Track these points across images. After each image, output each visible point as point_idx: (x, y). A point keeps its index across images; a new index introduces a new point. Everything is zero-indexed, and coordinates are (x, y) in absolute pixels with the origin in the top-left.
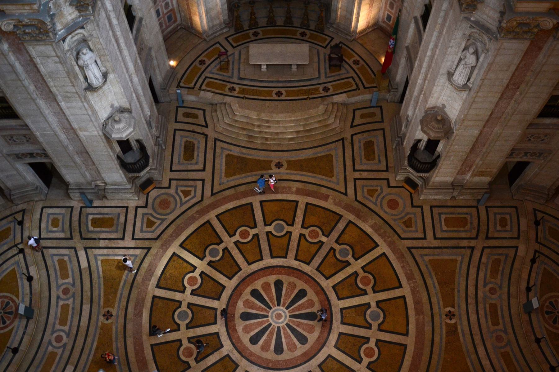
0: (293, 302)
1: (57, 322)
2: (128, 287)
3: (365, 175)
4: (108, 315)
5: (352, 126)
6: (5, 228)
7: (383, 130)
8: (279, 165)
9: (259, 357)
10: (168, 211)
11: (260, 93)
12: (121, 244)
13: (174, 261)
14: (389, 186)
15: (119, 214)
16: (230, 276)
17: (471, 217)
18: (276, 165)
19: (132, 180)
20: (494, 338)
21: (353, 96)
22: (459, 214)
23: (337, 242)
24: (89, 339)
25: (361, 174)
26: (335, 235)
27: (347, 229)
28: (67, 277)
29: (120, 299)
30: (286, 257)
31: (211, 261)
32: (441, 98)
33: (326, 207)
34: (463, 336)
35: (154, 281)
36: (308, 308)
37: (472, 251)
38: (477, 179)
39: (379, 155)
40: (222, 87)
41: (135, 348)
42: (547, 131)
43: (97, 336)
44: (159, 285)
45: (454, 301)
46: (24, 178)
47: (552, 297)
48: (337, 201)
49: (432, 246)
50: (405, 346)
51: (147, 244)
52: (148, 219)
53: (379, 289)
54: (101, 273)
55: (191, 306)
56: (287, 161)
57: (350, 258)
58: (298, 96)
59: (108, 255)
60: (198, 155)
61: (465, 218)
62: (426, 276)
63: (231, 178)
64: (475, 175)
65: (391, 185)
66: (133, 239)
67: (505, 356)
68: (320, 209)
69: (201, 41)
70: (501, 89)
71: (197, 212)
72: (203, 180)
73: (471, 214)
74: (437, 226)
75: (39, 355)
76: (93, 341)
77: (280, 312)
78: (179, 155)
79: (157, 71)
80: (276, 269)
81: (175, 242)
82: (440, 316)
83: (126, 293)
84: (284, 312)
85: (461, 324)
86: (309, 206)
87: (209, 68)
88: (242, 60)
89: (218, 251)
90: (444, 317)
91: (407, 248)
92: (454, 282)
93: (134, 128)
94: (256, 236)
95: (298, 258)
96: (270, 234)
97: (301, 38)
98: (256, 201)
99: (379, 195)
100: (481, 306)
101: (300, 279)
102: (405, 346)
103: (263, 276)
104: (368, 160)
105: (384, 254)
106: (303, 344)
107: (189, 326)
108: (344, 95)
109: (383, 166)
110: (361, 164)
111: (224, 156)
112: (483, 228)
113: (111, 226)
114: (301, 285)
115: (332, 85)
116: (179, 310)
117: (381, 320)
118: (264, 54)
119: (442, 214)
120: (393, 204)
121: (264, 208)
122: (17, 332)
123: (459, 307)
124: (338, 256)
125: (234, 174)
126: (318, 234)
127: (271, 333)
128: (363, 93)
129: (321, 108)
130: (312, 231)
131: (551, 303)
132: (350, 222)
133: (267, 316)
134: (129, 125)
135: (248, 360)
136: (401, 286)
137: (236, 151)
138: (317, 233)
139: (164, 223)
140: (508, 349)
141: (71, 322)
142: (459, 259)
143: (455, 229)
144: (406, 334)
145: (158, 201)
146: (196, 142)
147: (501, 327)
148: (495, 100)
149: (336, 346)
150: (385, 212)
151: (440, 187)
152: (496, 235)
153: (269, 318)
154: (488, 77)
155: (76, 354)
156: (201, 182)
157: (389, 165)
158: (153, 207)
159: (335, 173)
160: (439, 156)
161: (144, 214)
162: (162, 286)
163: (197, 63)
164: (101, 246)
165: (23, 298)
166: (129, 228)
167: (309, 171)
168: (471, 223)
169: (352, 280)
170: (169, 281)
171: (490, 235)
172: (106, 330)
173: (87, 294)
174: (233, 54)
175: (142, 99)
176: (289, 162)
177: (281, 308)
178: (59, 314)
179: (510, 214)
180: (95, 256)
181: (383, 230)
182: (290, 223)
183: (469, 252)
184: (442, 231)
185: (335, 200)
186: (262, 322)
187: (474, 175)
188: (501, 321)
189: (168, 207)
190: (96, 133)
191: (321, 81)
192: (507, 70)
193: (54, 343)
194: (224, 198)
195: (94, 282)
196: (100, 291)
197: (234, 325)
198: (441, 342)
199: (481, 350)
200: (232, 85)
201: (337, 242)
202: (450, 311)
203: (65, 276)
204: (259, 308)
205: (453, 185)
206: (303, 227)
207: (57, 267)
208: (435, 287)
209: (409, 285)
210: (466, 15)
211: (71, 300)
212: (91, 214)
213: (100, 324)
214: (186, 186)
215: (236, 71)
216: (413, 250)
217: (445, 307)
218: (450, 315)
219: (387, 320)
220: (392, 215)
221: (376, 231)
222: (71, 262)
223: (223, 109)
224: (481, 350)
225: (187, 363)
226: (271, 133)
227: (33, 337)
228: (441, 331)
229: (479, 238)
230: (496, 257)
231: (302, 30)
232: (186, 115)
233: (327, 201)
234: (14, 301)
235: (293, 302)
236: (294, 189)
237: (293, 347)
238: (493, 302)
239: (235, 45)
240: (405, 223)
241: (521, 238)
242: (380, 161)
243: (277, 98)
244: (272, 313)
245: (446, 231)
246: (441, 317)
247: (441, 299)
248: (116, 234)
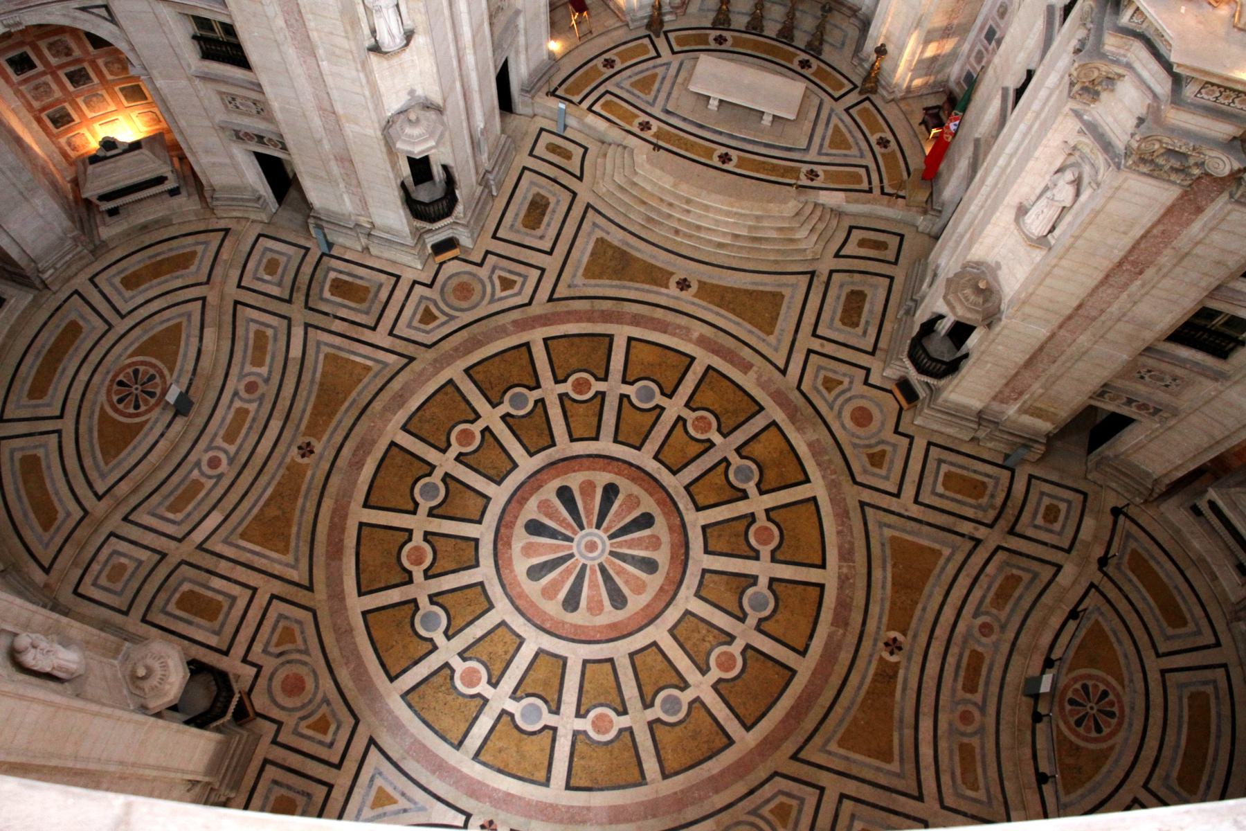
0: (624, 530)
1: (222, 433)
2: (355, 412)
3: (829, 349)
4: (307, 450)
5: (837, 255)
6: (188, 250)
7: (892, 279)
8: (683, 285)
9: (533, 604)
10: (465, 305)
11: (690, 147)
12: (368, 336)
13: (446, 394)
14: (866, 383)
15: (381, 286)
16: (532, 450)
17: (996, 486)
18: (678, 283)
19: (419, 236)
20: (957, 714)
21: (856, 201)
22: (975, 472)
23: (738, 450)
24: (264, 479)
25: (822, 345)
26: (739, 437)
28: (261, 364)
29: (335, 429)
30: (639, 448)
31: (508, 414)
32: (996, 250)
33: (740, 383)
34: (904, 689)
35: (401, 416)
36: (647, 548)
37: (975, 547)
38: (1026, 419)
39: (867, 322)
40: (629, 118)
41: (332, 518)
42: (1179, 372)
43: (278, 478)
44: (408, 427)
45: (909, 624)
46: (241, 174)
47: (1090, 677)
48: (765, 378)
49: (906, 514)
50: (794, 672)
51: (410, 349)
52: (427, 310)
53: (782, 558)
54: (318, 375)
55: (448, 480)
56: (699, 282)
57: (751, 487)
58: (758, 171)
59: (339, 348)
60: (548, 225)
61: (983, 483)
62: (876, 563)
63: (593, 282)
64: (1026, 412)
65: (871, 381)
66: (391, 334)
67: (966, 753)
68: (728, 383)
69: (619, 24)
70: (1106, 265)
71: (515, 322)
72: (543, 270)
73: (997, 480)
74: (928, 481)
75: (175, 479)
76: (269, 484)
77: (596, 539)
78: (517, 215)
79: (522, 57)
80: (615, 463)
81: (458, 362)
82: (876, 640)
83: (348, 423)
84: (603, 543)
85: (907, 669)
86: (711, 371)
87: (617, 78)
88: (680, 80)
89: (525, 400)
90: (881, 645)
91: (860, 502)
92: (921, 591)
93: (438, 143)
94: (601, 395)
95: (660, 457)
96: (625, 400)
97: (799, 69)
98: (621, 333)
99: (844, 392)
100: (954, 650)
101: (651, 495)
102: (794, 672)
103: (589, 469)
104: (844, 324)
105: (814, 499)
106: (616, 608)
107: (435, 512)
108: (841, 195)
109: (868, 344)
110: (830, 326)
111: (594, 239)
112: (1011, 512)
113: (362, 300)
114: (648, 504)
115: (825, 171)
116: (427, 480)
117: (767, 613)
118: (719, 79)
119: (944, 462)
120: (862, 418)
121: (632, 351)
122: (152, 428)
123: (915, 636)
124: (731, 477)
125: (600, 276)
126: (710, 428)
127: (569, 571)
128: (875, 201)
129: (791, 206)
130: (702, 418)
131: (1085, 687)
132: (774, 423)
133: (571, 540)
134: (431, 134)
135: (513, 603)
136: (823, 566)
137: (616, 237)
138: (710, 424)
139: (452, 323)
140: (975, 741)
141: (244, 440)
142: (946, 552)
143: (959, 497)
144: (803, 653)
145: (455, 281)
146: (552, 200)
147: (977, 698)
148: (1091, 283)
149: (672, 631)
150: (843, 427)
151: (956, 414)
152: (1030, 532)
153: (574, 544)
154: (1086, 234)
155: (233, 497)
156: (539, 272)
157: (880, 345)
158: (442, 291)
159: (777, 331)
160: (966, 356)
161: (422, 298)
162: (412, 430)
163: (599, 62)
164: (333, 328)
165: (179, 376)
166: (391, 313)
167: (733, 311)
168: (992, 496)
169: (741, 526)
170: (427, 426)
171: (1018, 529)
172: (294, 474)
173: (284, 403)
174: (668, 64)
175: (476, 97)
176: (702, 284)
177: (600, 532)
178: (228, 421)
179: (1069, 502)
180: (319, 343)
181: (826, 458)
182: (668, 392)
183: (970, 544)
184: (934, 493)
185: (760, 376)
186: (558, 546)
187: (1023, 411)
188: (981, 689)
189: (466, 298)
190: (370, 132)
191: (807, 158)
192: (1125, 233)
193: (205, 468)
194: (568, 313)
195: (302, 386)
196: (306, 406)
197: (510, 537)
198: (859, 688)
199: (926, 724)
200: (647, 118)
201: (738, 450)
202: (895, 640)
203: (258, 362)
204: (562, 522)
205: (980, 418)
206: (687, 405)
207: (251, 342)
208: (883, 587)
209: (840, 567)
210: (1077, 107)
211: (255, 405)
212: (335, 270)
213: (288, 460)
214: (510, 272)
215: (663, 95)
216: (867, 509)
217: (889, 629)
218: (893, 646)
219: (778, 616)
220: (853, 435)
221: (814, 455)
222: (275, 339)
223: (618, 155)
224: (926, 724)
225: (410, 573)
226: (688, 224)
227: (175, 448)
228: (867, 670)
229: (997, 527)
230: (1015, 572)
231: (807, 57)
232: (553, 148)
233: (746, 373)
234: (162, 376)
235: (624, 530)
236: (696, 335)
237: (595, 608)
238: (980, 649)
239: (676, 48)
240: (871, 457)
241: (1074, 553)
242: (865, 333)
243: (719, 165)
244: (583, 537)
245: (941, 496)
246: (875, 645)
247: (887, 612)
248: (364, 316)
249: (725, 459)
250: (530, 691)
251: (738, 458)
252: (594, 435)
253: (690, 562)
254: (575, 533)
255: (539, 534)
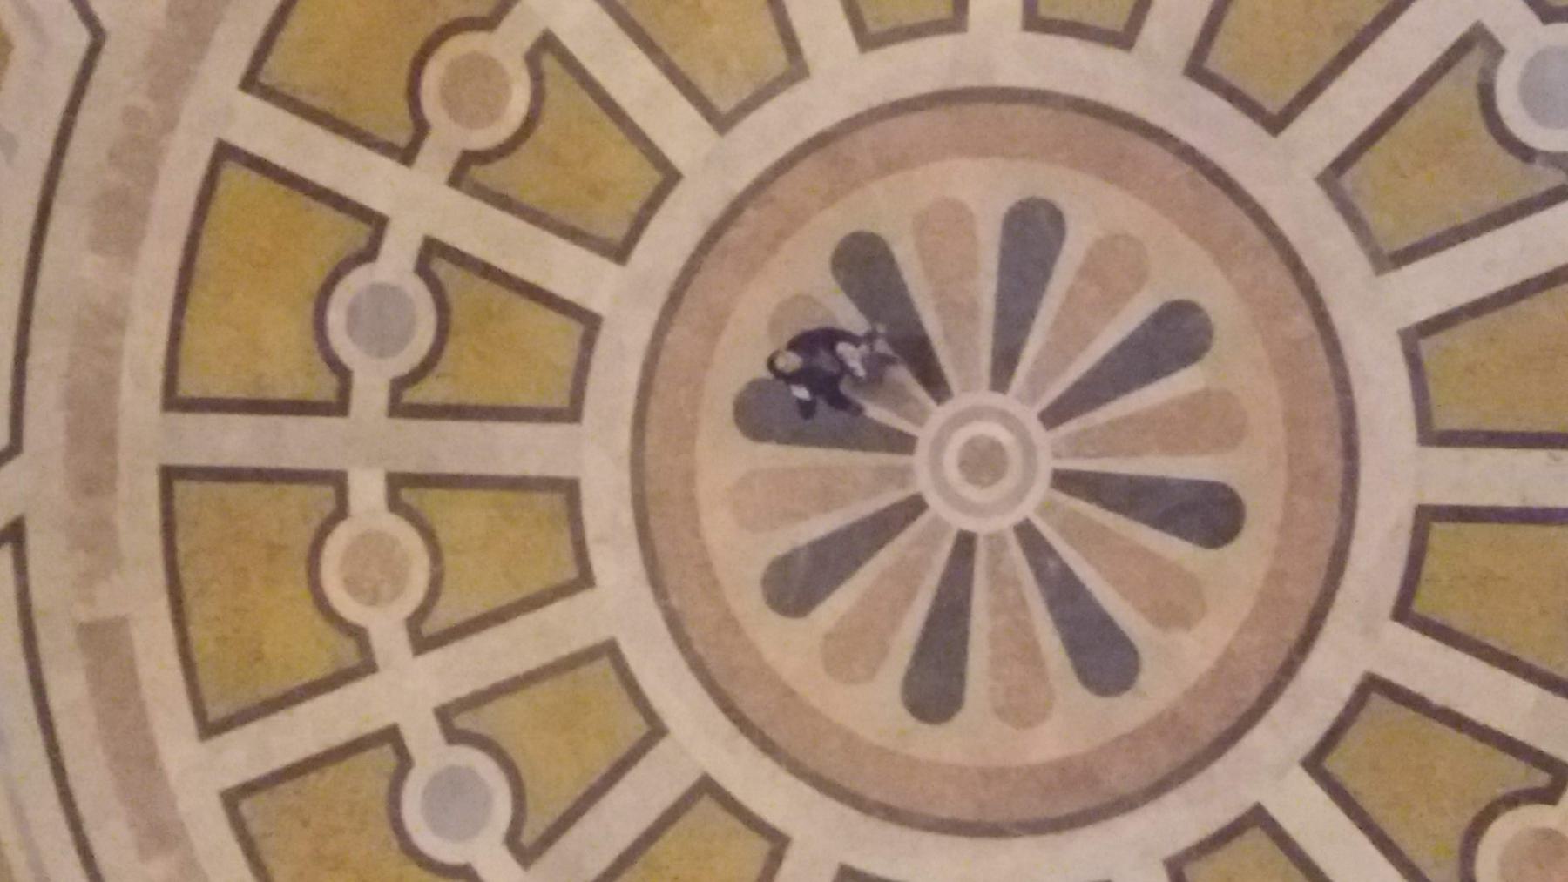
23: (339, 406)
26: (300, 442)
27: (220, 390)
77: (953, 473)
84: (939, 445)
101: (689, 478)
127: (1108, 440)
130: (352, 585)
132: (174, 401)
133: (1026, 532)
138: (351, 554)
153: (1027, 509)
177: (922, 483)
201: (339, 406)
249: (398, 408)
250: (1513, 162)
251: (359, 381)
252: (706, 805)
253: (740, 184)
254: (997, 540)
255: (1106, 622)
